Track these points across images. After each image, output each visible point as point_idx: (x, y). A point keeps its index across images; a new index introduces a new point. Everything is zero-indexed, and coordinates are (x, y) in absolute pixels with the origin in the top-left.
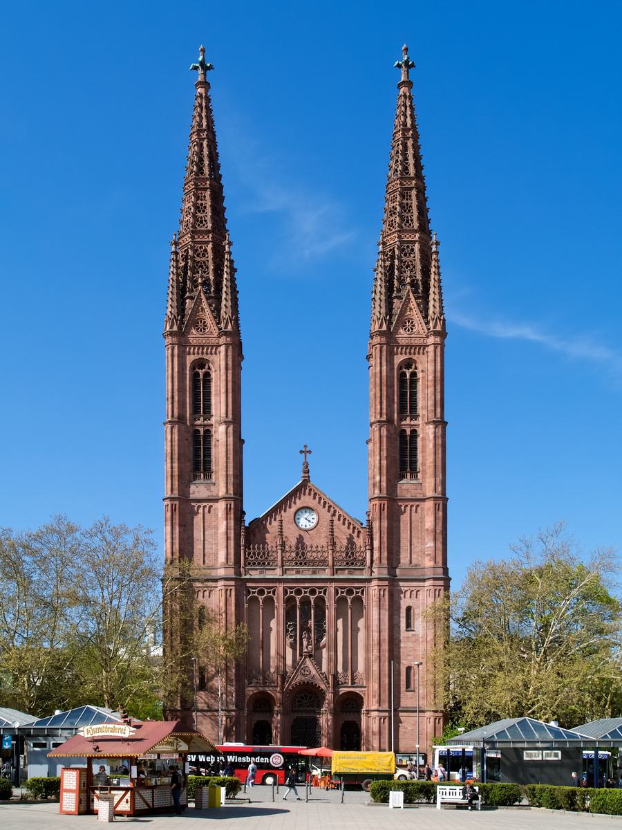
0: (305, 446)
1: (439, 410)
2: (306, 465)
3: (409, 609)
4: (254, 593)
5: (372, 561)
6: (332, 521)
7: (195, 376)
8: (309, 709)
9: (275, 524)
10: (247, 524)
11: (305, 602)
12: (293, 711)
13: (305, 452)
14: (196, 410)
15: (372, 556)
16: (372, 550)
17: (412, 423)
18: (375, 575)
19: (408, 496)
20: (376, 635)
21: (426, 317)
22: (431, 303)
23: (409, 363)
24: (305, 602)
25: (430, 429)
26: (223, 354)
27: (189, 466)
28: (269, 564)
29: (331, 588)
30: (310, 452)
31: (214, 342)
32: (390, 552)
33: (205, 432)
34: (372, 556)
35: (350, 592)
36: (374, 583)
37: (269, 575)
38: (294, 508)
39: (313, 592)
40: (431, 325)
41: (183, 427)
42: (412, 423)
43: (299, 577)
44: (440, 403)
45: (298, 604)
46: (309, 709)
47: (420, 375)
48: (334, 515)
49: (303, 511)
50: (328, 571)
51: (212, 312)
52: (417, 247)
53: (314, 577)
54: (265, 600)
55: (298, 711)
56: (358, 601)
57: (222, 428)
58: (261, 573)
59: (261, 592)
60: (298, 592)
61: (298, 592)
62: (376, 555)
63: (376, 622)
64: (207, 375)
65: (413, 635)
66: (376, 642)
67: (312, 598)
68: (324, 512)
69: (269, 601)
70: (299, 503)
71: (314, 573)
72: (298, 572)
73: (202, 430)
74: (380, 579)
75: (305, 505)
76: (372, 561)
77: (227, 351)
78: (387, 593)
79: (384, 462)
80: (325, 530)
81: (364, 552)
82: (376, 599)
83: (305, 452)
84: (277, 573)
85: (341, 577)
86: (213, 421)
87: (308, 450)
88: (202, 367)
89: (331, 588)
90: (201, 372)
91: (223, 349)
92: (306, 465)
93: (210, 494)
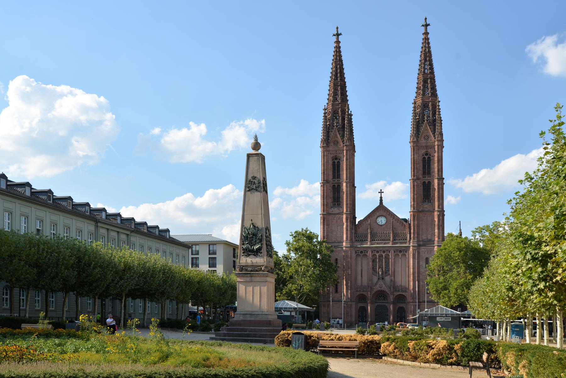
1: (440, 173)
2: (381, 198)
5: (410, 238)
7: (334, 162)
11: (381, 256)
14: (334, 177)
15: (410, 236)
16: (410, 234)
17: (428, 178)
18: (411, 244)
20: (411, 270)
21: (434, 134)
25: (436, 181)
27: (330, 200)
28: (365, 240)
32: (418, 234)
34: (410, 236)
36: (411, 248)
38: (376, 217)
40: (436, 136)
41: (328, 185)
42: (428, 178)
44: (440, 170)
48: (394, 218)
50: (391, 243)
51: (341, 137)
52: (430, 104)
57: (344, 184)
59: (362, 252)
62: (412, 236)
63: (411, 265)
66: (412, 273)
68: (389, 217)
70: (378, 214)
71: (385, 244)
72: (378, 244)
73: (336, 185)
76: (410, 238)
77: (346, 153)
78: (416, 252)
79: (416, 196)
82: (411, 255)
84: (368, 245)
87: (382, 191)
91: (345, 151)
92: (381, 198)
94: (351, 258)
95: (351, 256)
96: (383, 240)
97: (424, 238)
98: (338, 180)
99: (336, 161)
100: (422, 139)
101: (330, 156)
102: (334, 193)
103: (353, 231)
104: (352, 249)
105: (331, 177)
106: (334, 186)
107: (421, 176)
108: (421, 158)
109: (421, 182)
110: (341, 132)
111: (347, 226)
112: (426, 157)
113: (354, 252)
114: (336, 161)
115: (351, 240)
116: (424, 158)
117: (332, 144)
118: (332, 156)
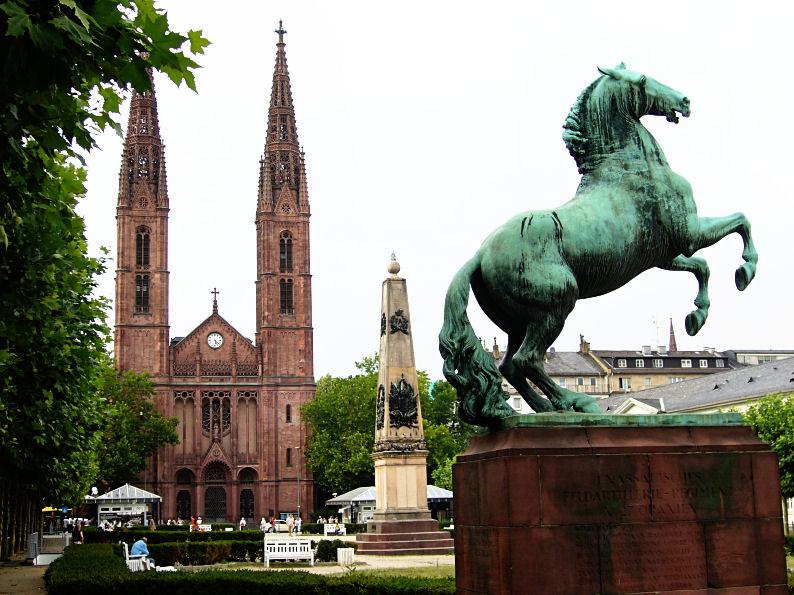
2: (215, 302)
3: (288, 407)
6: (234, 343)
7: (139, 237)
9: (194, 344)
11: (216, 401)
13: (215, 293)
14: (139, 262)
19: (287, 326)
20: (266, 426)
22: (301, 194)
23: (286, 234)
24: (216, 401)
26: (159, 223)
27: (133, 302)
29: (234, 393)
31: (153, 214)
37: (191, 382)
38: (206, 334)
39: (221, 395)
41: (129, 274)
43: (211, 383)
47: (294, 242)
55: (210, 483)
56: (254, 400)
58: (184, 380)
60: (211, 394)
61: (211, 394)
64: (147, 237)
67: (221, 399)
68: (227, 335)
69: (191, 401)
70: (210, 329)
71: (222, 380)
72: (210, 380)
74: (268, 386)
80: (228, 349)
83: (215, 293)
85: (241, 384)
86: (150, 270)
88: (143, 230)
89: (234, 393)
92: (215, 302)
94: (168, 405)
95: (168, 401)
96: (220, 374)
99: (143, 235)
100: (280, 210)
101: (134, 226)
103: (172, 358)
105: (134, 262)
107: (278, 270)
108: (278, 240)
111: (162, 348)
112: (286, 240)
114: (143, 235)
116: (282, 241)
117: (137, 205)
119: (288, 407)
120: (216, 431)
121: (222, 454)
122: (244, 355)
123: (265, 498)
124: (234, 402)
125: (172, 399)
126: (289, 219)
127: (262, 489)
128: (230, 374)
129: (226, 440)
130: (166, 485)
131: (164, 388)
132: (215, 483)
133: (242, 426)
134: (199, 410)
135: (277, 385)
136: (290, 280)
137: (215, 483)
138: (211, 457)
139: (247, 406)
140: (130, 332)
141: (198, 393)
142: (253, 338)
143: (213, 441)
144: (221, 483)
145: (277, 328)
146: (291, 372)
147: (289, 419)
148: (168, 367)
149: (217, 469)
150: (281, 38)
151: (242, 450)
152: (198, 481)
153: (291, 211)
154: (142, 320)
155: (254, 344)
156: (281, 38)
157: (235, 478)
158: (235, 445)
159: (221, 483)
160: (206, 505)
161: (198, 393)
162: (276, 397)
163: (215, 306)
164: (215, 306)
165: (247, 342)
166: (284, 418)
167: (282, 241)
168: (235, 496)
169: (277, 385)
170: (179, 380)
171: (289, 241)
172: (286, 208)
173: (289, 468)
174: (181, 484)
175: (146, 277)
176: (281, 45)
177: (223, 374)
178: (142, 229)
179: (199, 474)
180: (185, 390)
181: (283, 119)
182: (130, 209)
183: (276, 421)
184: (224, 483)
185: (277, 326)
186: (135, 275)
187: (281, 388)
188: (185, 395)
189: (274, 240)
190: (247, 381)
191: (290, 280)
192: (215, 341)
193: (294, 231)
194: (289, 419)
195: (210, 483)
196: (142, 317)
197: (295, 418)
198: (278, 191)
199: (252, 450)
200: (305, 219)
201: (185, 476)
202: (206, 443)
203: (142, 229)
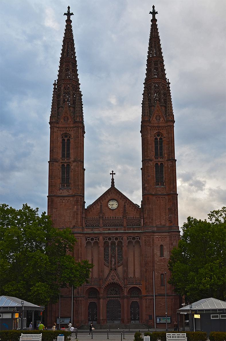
0: (113, 171)
2: (113, 179)
4: (89, 240)
6: (125, 205)
7: (64, 140)
8: (115, 296)
10: (86, 207)
11: (113, 243)
12: (108, 297)
13: (113, 174)
14: (63, 155)
17: (161, 160)
19: (160, 193)
23: (159, 134)
24: (113, 243)
29: (125, 238)
30: (115, 174)
33: (67, 165)
35: (134, 238)
38: (107, 200)
39: (116, 239)
45: (110, 245)
46: (115, 296)
49: (112, 201)
53: (117, 232)
54: (94, 243)
55: (110, 297)
56: (138, 242)
58: (92, 230)
60: (110, 239)
61: (110, 239)
64: (68, 140)
65: (164, 259)
67: (116, 242)
69: (96, 243)
71: (117, 230)
72: (109, 230)
73: (66, 165)
75: (112, 198)
81: (140, 221)
88: (66, 136)
89: (125, 238)
90: (66, 139)
92: (113, 179)
93: (69, 194)
95: (81, 243)
96: (115, 226)
97: (157, 224)
98: (67, 159)
102: (63, 173)
103: (84, 216)
104: (82, 235)
106: (63, 165)
107: (153, 157)
109: (153, 163)
110: (72, 109)
111: (77, 209)
113: (84, 239)
114: (66, 139)
115: (82, 225)
116: (156, 139)
117: (62, 120)
118: (62, 133)
119: (162, 246)
120: (113, 263)
121: (117, 278)
122: (132, 214)
123: (146, 307)
124: (125, 243)
125: (84, 242)
126: (160, 125)
127: (144, 301)
128: (122, 226)
129: (120, 269)
130: (80, 299)
131: (79, 235)
132: (114, 297)
133: (131, 259)
134: (102, 249)
135: (154, 232)
136: (162, 164)
137: (114, 297)
138: (110, 280)
139: (134, 246)
140: (56, 200)
141: (101, 238)
142: (139, 204)
143: (111, 270)
144: (117, 297)
145: (153, 195)
146: (163, 223)
147: (162, 255)
148: (82, 222)
149: (114, 287)
150: (154, 16)
151: (131, 275)
152: (101, 296)
153: (162, 119)
154: (65, 193)
155: (140, 207)
156: (154, 16)
157: (126, 294)
158: (126, 272)
159: (117, 297)
160: (108, 312)
161: (101, 238)
162: (153, 240)
163: (113, 182)
164: (113, 182)
165: (136, 206)
166: (159, 254)
167: (156, 139)
168: (126, 305)
169: (154, 232)
170: (89, 230)
171: (161, 139)
172: (158, 118)
173: (163, 287)
174: (91, 298)
175: (68, 165)
176: (154, 20)
177: (117, 226)
178: (66, 135)
179: (102, 291)
180: (93, 236)
181: (156, 64)
182: (58, 123)
183: (153, 256)
184: (120, 297)
185: (153, 193)
186: (61, 165)
187: (156, 234)
188: (92, 239)
189: (150, 138)
190: (134, 230)
191: (162, 164)
192: (113, 205)
193: (164, 132)
194: (162, 255)
195: (110, 297)
196: (65, 191)
197: (166, 254)
198: (153, 108)
199: (137, 275)
200: (171, 124)
201: (93, 292)
202: (107, 270)
203: (66, 135)
